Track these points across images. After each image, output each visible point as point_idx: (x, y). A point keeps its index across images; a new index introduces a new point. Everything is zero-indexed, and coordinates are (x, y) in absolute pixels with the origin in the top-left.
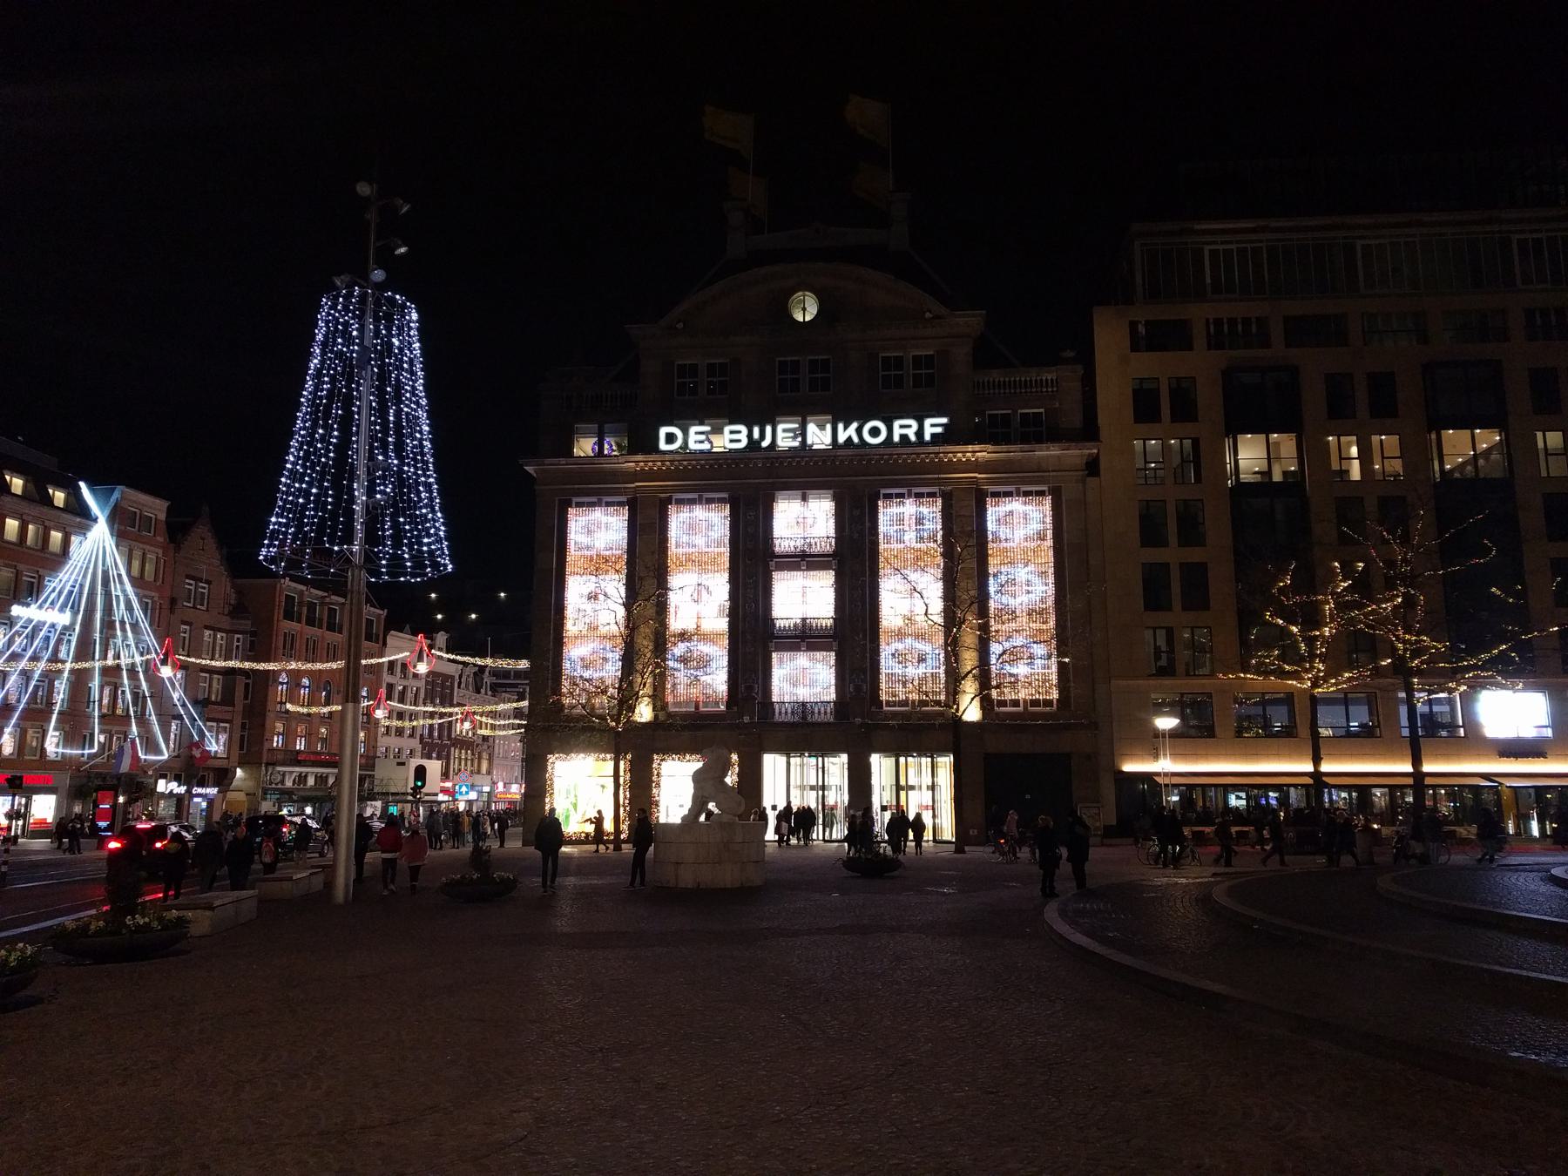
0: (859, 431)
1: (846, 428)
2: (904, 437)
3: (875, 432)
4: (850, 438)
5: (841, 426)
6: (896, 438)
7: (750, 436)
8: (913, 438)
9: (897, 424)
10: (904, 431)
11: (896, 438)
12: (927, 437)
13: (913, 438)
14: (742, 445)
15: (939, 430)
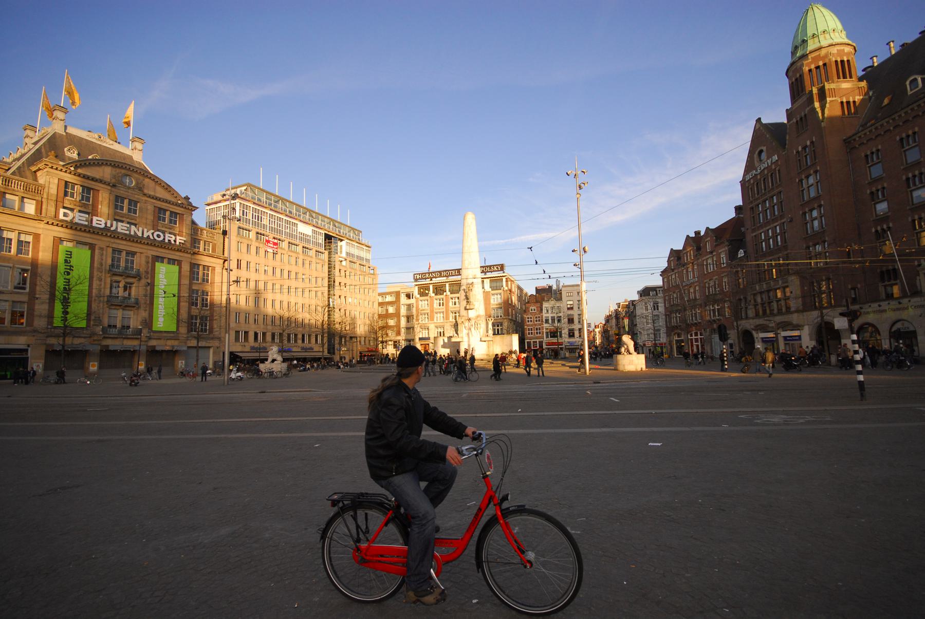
0: (153, 234)
1: (147, 232)
2: (169, 240)
3: (159, 236)
4: (149, 236)
5: (145, 230)
6: (167, 241)
7: (106, 224)
8: (173, 242)
9: (167, 235)
10: (170, 239)
11: (167, 241)
12: (178, 243)
13: (173, 242)
14: (103, 226)
15: (183, 242)
